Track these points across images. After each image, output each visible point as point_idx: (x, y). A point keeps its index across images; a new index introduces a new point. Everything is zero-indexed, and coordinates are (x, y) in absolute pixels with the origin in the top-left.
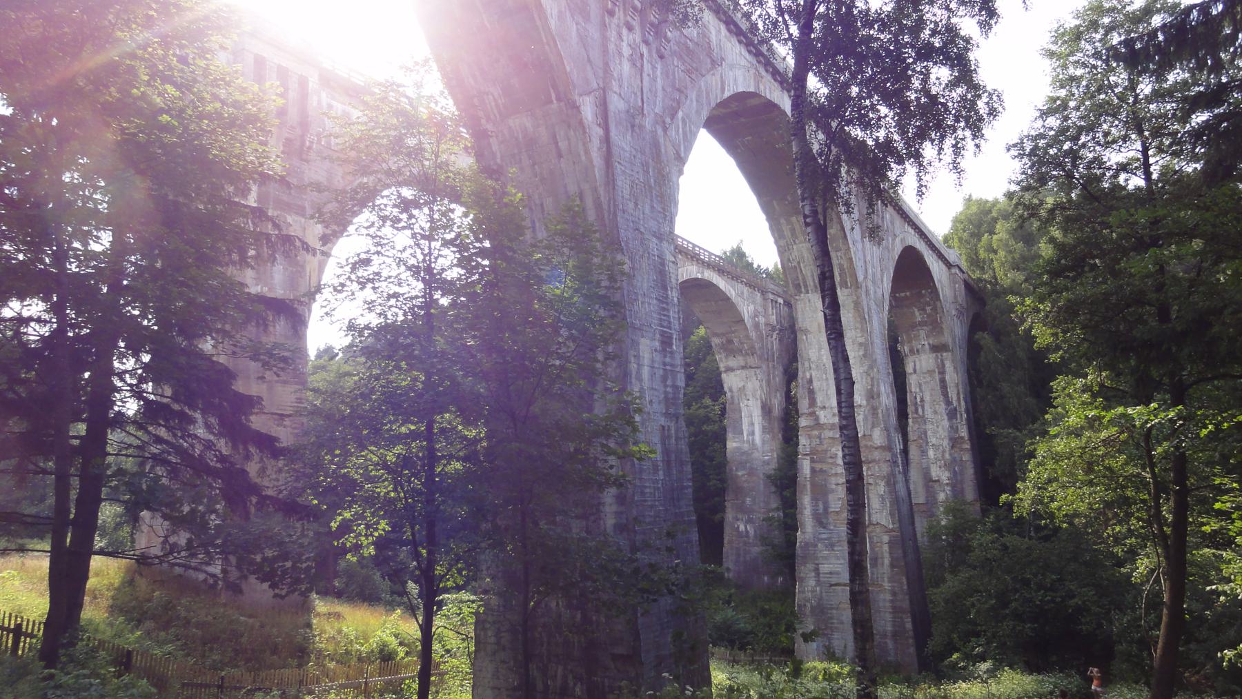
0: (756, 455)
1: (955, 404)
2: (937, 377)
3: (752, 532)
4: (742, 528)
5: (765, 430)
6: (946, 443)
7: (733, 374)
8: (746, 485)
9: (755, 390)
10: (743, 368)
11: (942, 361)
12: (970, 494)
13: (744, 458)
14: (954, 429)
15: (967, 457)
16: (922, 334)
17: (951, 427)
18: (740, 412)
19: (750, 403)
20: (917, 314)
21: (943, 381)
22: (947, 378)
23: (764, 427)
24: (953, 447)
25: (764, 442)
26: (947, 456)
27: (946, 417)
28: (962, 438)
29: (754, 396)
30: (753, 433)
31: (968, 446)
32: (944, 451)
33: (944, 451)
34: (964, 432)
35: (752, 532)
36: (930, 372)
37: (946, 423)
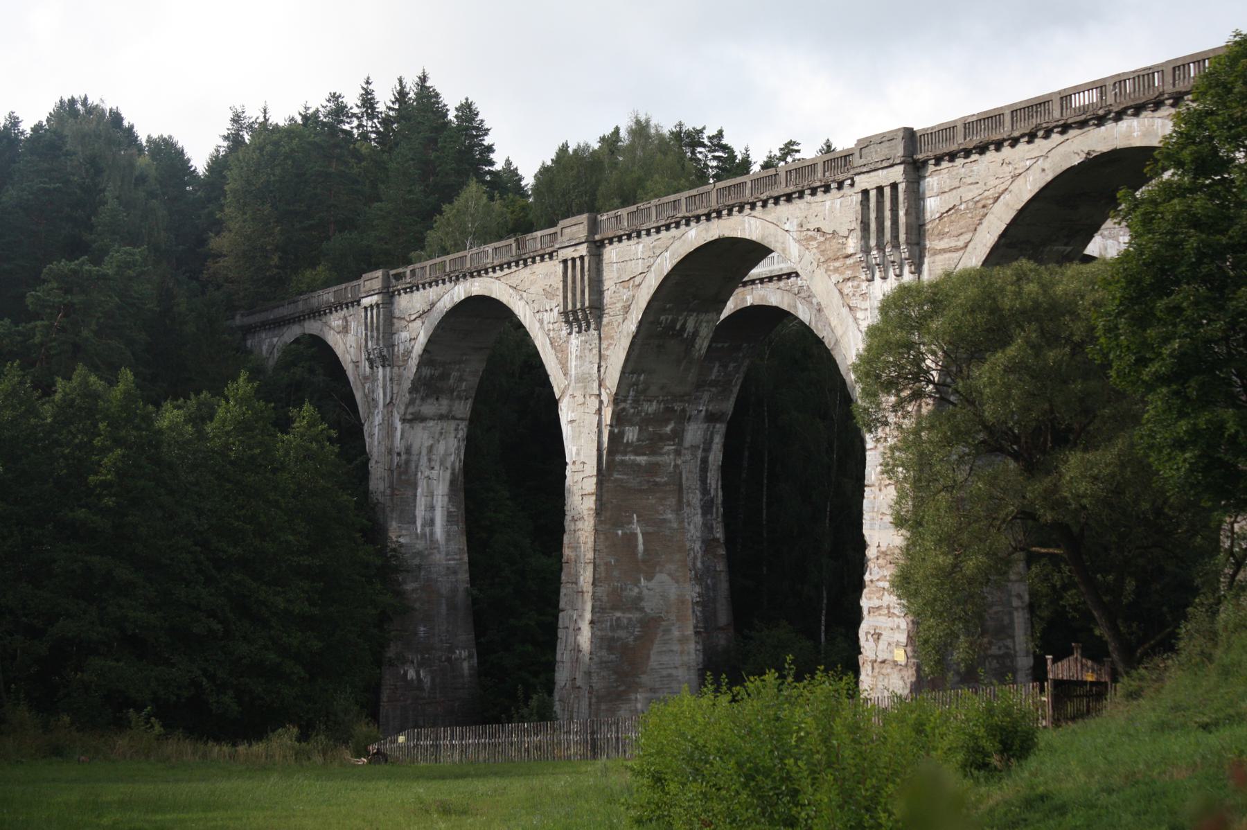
0: (439, 558)
1: (712, 492)
2: (700, 454)
3: (427, 681)
4: (411, 674)
5: (450, 518)
6: (697, 546)
7: (422, 425)
8: (417, 605)
9: (447, 454)
10: (441, 417)
11: (712, 433)
12: (723, 618)
13: (417, 561)
14: (708, 527)
15: (721, 567)
16: (706, 396)
17: (705, 524)
18: (415, 486)
19: (434, 474)
20: (715, 370)
21: (705, 461)
22: (711, 458)
23: (449, 514)
24: (705, 552)
25: (448, 535)
26: (699, 565)
27: (699, 511)
28: (717, 540)
29: (442, 464)
30: (431, 522)
31: (722, 551)
32: (695, 558)
33: (695, 558)
34: (719, 534)
35: (427, 681)
36: (694, 448)
37: (698, 519)
